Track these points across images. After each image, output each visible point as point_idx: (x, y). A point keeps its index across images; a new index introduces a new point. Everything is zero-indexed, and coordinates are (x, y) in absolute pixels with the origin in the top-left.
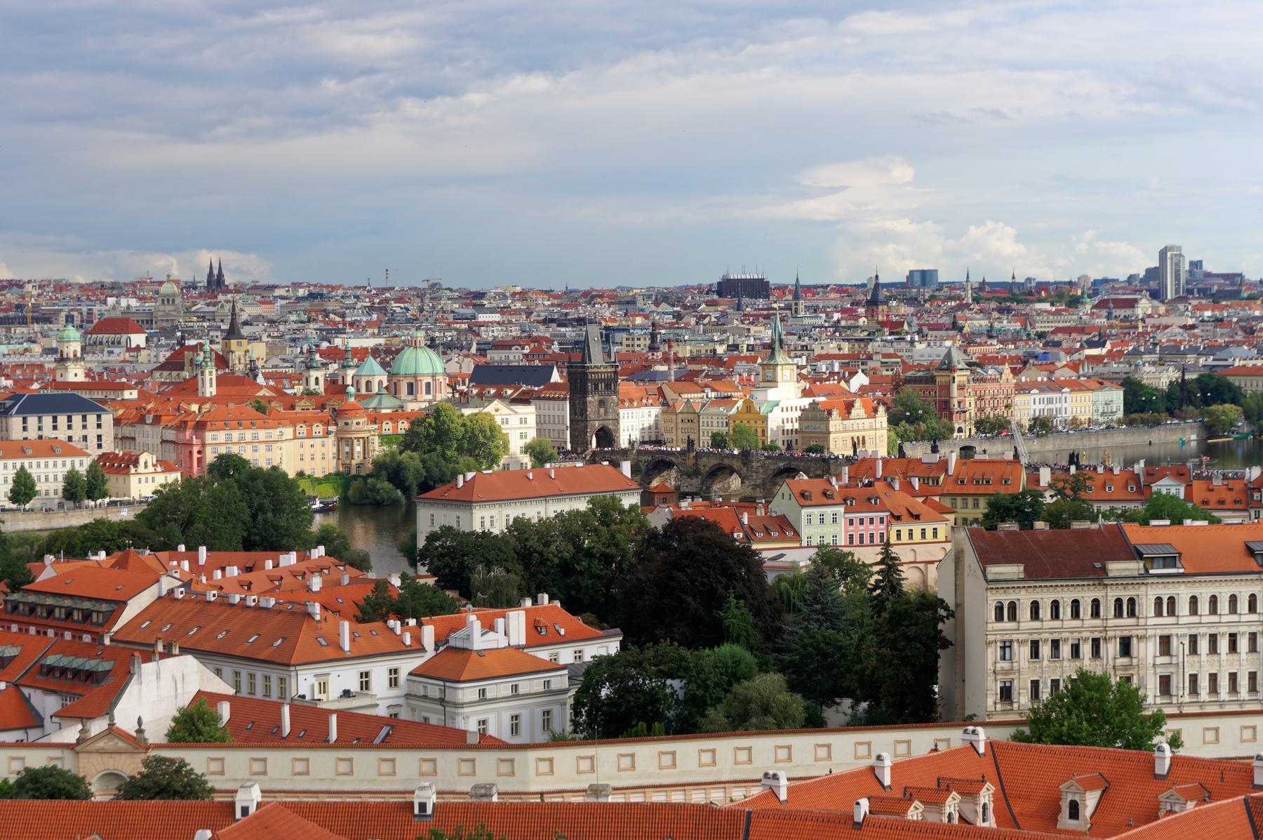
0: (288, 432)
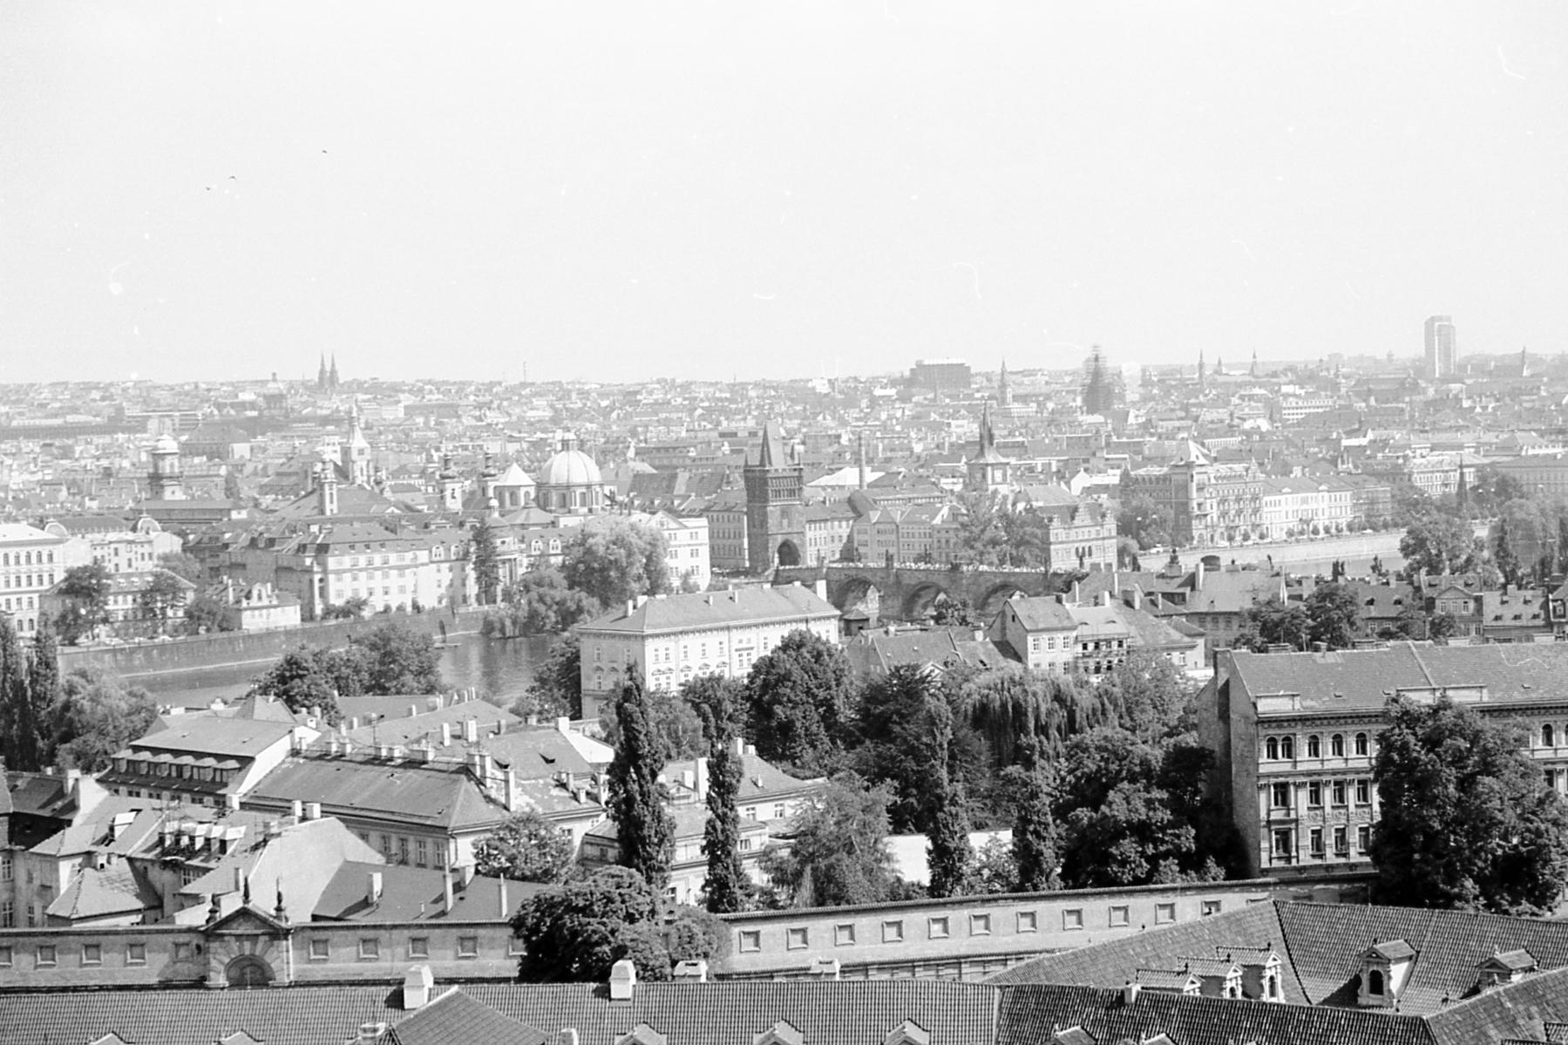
0: (423, 556)
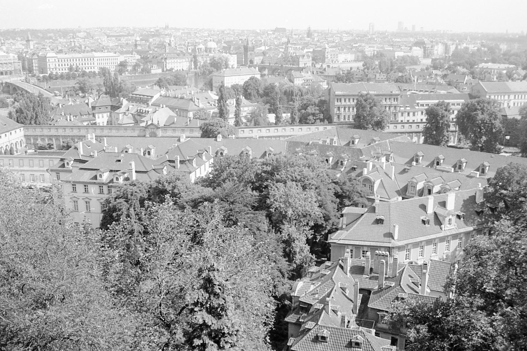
0: (184, 60)
